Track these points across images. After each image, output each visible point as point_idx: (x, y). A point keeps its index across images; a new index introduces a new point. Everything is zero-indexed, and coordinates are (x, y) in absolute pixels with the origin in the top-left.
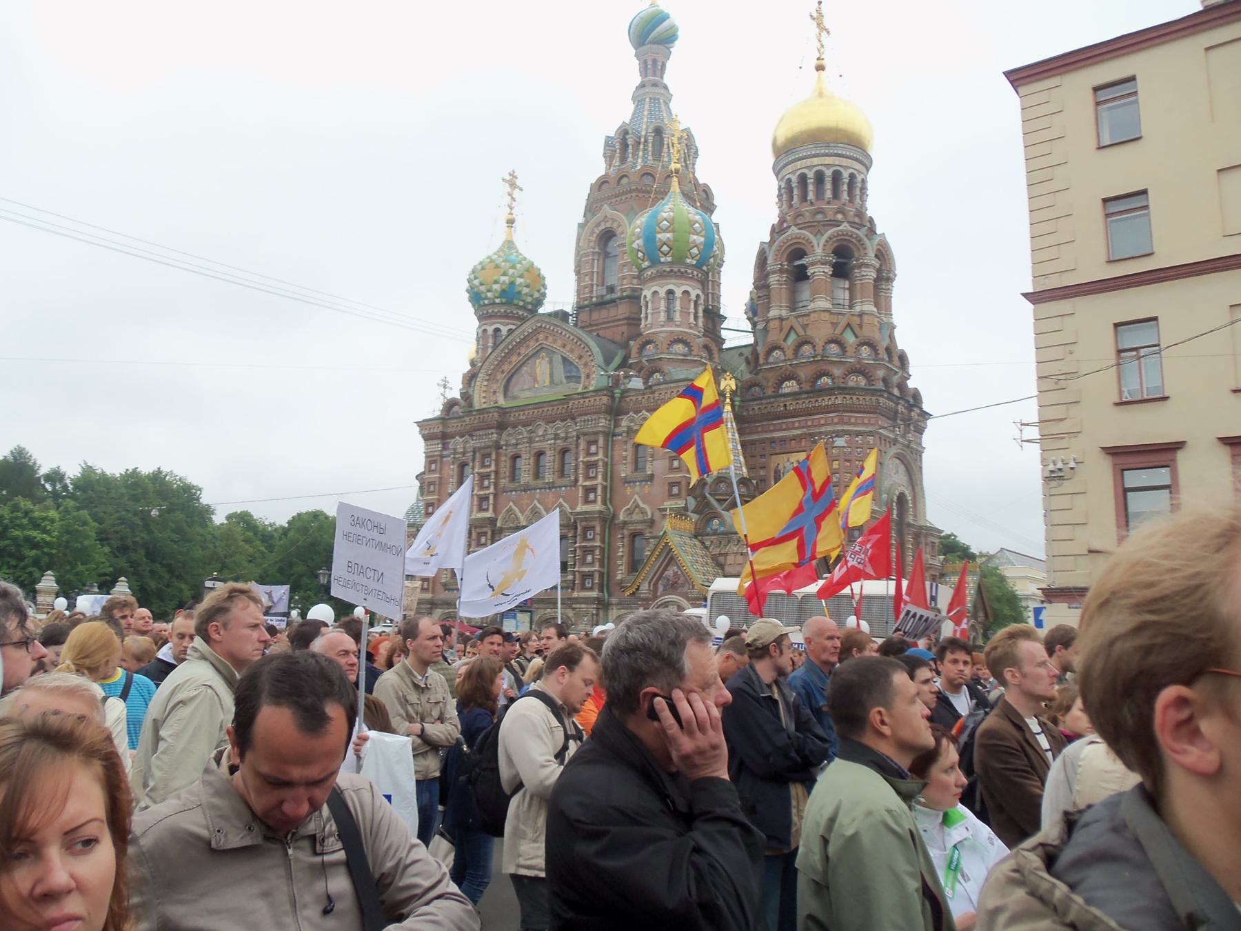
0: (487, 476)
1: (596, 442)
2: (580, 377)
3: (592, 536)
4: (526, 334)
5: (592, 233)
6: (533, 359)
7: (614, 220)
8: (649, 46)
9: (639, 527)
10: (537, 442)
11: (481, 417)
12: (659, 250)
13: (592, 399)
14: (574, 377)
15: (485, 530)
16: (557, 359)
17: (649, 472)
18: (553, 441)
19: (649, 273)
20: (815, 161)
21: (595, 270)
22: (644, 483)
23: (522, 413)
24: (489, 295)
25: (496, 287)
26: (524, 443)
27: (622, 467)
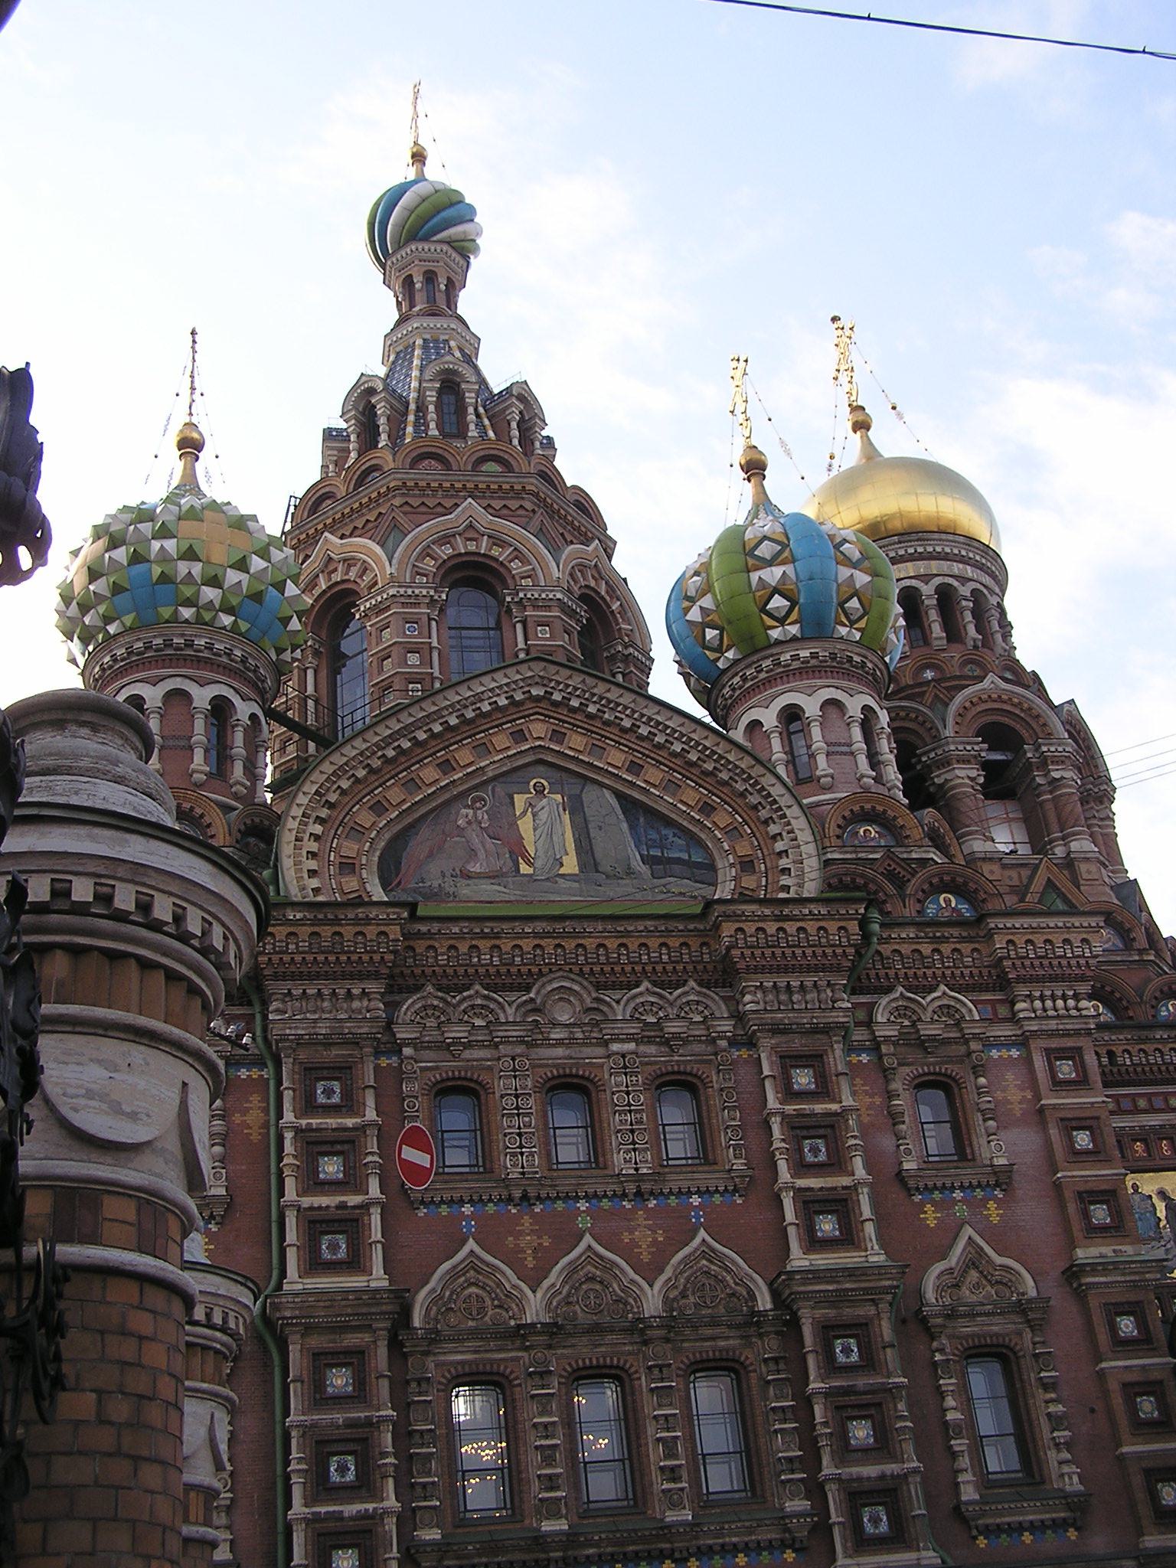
0: (345, 1144)
1: (814, 1060)
2: (712, 867)
3: (855, 1357)
4: (486, 707)
5: (426, 553)
6: (500, 790)
7: (497, 541)
8: (445, 247)
9: (998, 1326)
10: (560, 1043)
11: (327, 931)
12: (841, 604)
13: (811, 927)
14: (679, 861)
15: (352, 1340)
16: (601, 803)
17: (1002, 1161)
18: (632, 1046)
19: (804, 653)
20: (970, 572)
21: (435, 644)
22: (979, 1193)
23: (484, 945)
24: (210, 594)
25: (243, 577)
26: (506, 1040)
27: (887, 1142)
